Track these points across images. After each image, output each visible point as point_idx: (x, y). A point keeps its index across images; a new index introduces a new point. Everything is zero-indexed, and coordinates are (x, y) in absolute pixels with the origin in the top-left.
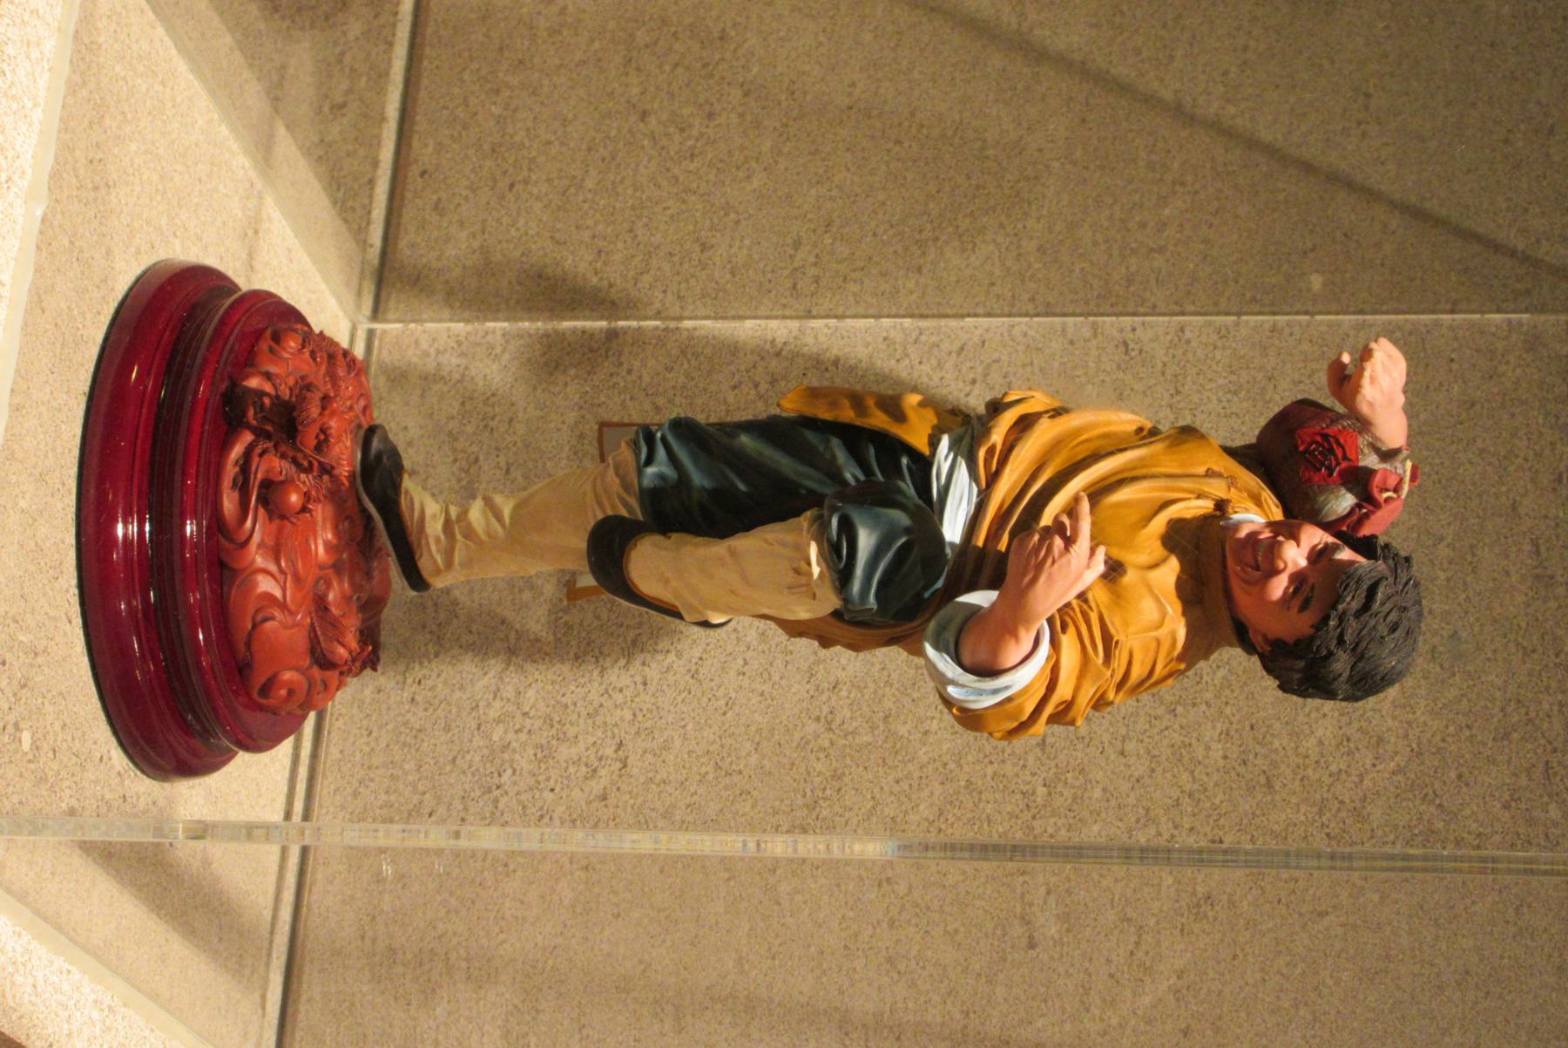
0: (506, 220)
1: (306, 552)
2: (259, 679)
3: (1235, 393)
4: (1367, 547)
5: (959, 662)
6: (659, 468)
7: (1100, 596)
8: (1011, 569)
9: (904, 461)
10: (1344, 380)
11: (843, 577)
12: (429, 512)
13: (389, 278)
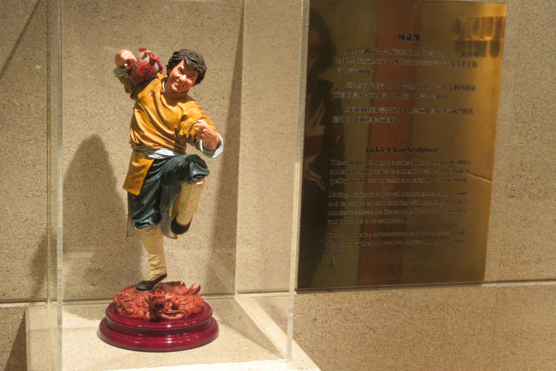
0: (18, 272)
3: (73, 87)
9: (154, 165)
12: (155, 274)
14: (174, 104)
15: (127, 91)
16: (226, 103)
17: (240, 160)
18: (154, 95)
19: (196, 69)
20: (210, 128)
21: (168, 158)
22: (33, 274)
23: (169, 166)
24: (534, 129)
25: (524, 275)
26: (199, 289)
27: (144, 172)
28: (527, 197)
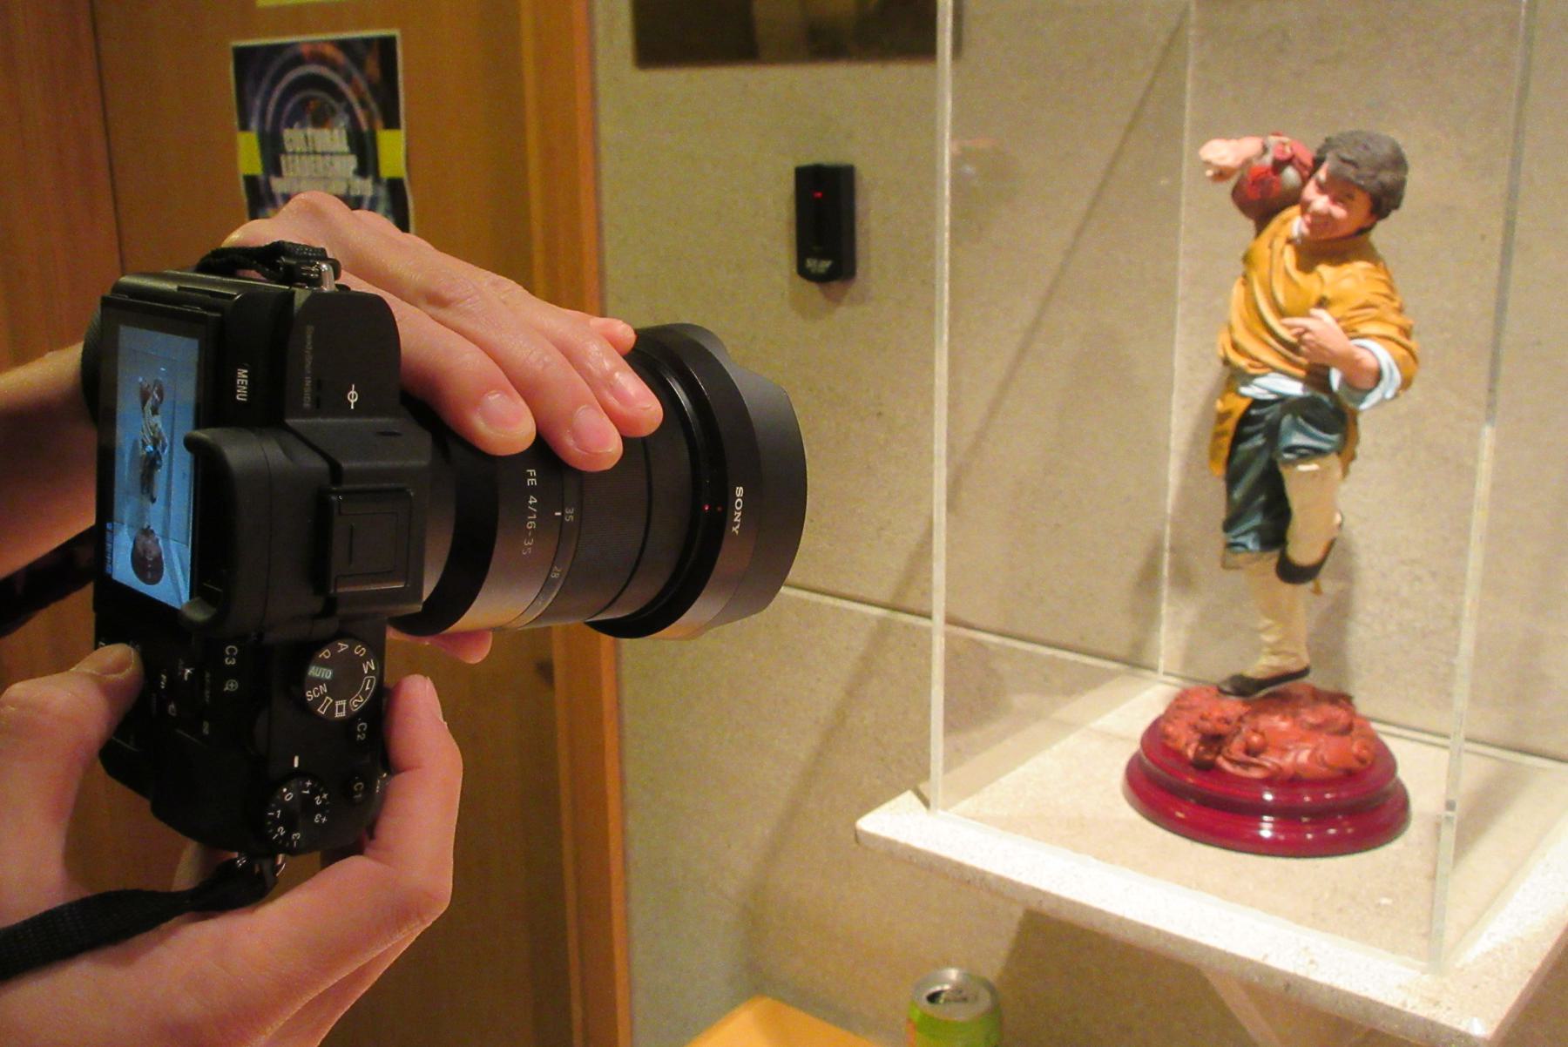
1: (1284, 734)
2: (1356, 765)
4: (1318, 163)
5: (1370, 391)
6: (1250, 542)
7: (1338, 310)
8: (1318, 361)
9: (1253, 412)
10: (1222, 174)
11: (1318, 452)
13: (1136, 661)
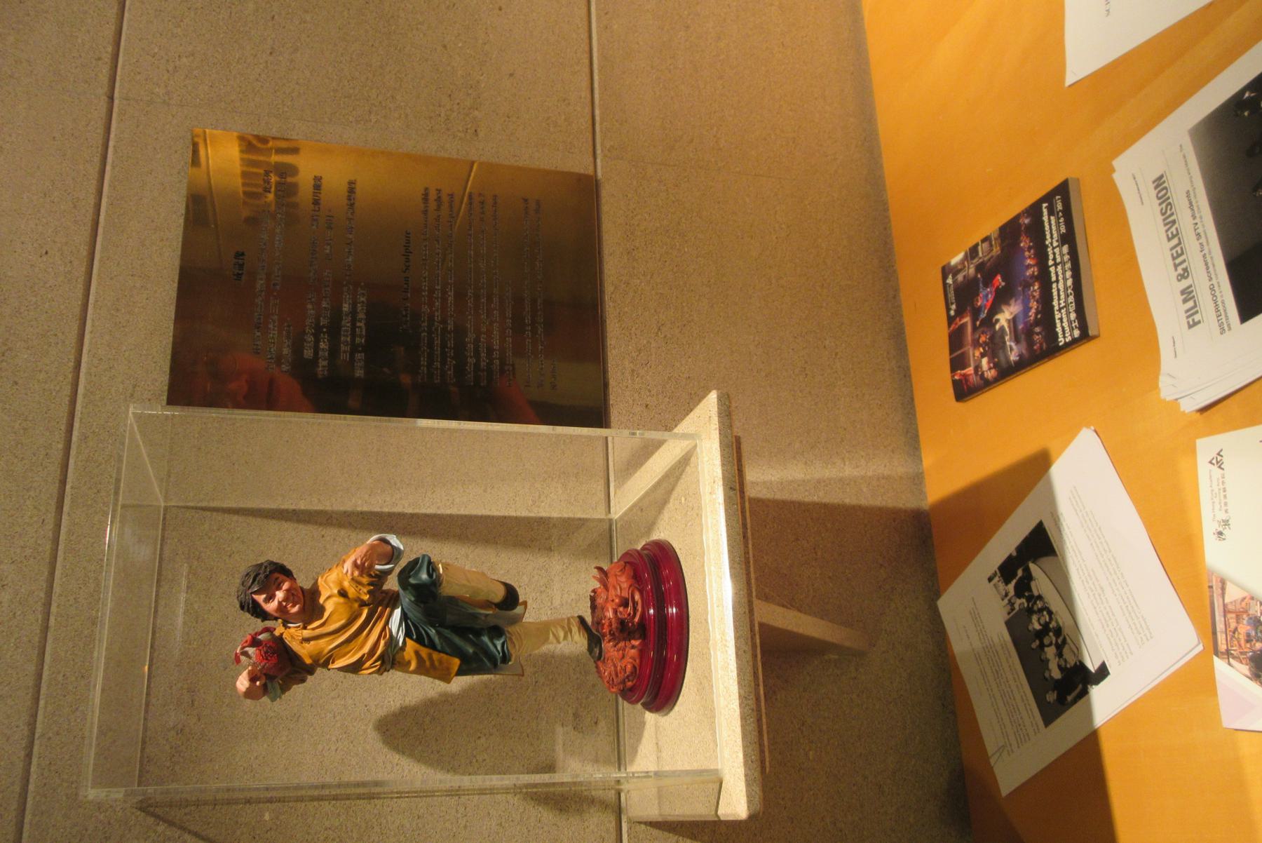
14: (322, 609)
15: (303, 681)
16: (330, 532)
17: (416, 511)
18: (307, 640)
19: (266, 577)
20: (357, 554)
21: (404, 617)
22: (580, 812)
23: (414, 614)
24: (380, 98)
25: (585, 123)
26: (600, 569)
27: (424, 652)
28: (476, 113)
